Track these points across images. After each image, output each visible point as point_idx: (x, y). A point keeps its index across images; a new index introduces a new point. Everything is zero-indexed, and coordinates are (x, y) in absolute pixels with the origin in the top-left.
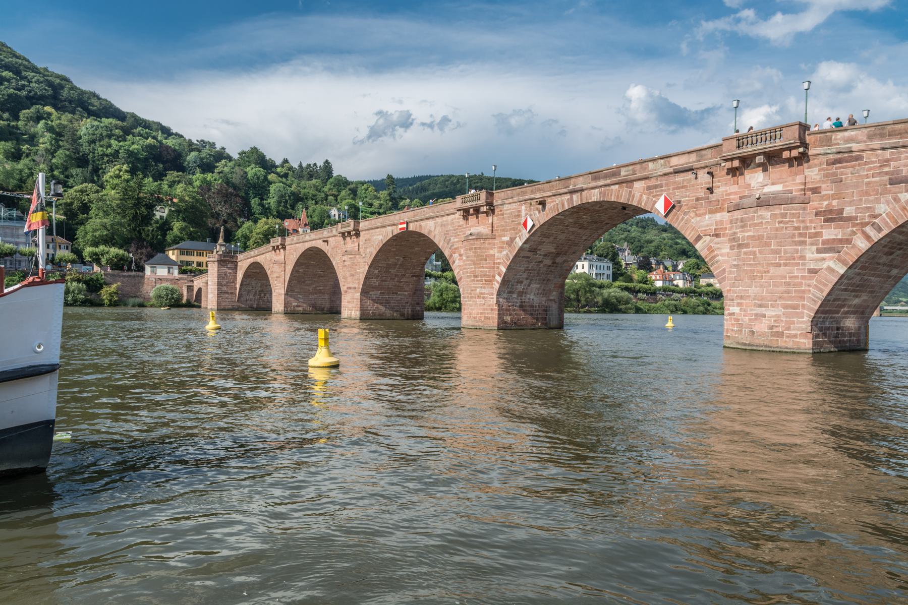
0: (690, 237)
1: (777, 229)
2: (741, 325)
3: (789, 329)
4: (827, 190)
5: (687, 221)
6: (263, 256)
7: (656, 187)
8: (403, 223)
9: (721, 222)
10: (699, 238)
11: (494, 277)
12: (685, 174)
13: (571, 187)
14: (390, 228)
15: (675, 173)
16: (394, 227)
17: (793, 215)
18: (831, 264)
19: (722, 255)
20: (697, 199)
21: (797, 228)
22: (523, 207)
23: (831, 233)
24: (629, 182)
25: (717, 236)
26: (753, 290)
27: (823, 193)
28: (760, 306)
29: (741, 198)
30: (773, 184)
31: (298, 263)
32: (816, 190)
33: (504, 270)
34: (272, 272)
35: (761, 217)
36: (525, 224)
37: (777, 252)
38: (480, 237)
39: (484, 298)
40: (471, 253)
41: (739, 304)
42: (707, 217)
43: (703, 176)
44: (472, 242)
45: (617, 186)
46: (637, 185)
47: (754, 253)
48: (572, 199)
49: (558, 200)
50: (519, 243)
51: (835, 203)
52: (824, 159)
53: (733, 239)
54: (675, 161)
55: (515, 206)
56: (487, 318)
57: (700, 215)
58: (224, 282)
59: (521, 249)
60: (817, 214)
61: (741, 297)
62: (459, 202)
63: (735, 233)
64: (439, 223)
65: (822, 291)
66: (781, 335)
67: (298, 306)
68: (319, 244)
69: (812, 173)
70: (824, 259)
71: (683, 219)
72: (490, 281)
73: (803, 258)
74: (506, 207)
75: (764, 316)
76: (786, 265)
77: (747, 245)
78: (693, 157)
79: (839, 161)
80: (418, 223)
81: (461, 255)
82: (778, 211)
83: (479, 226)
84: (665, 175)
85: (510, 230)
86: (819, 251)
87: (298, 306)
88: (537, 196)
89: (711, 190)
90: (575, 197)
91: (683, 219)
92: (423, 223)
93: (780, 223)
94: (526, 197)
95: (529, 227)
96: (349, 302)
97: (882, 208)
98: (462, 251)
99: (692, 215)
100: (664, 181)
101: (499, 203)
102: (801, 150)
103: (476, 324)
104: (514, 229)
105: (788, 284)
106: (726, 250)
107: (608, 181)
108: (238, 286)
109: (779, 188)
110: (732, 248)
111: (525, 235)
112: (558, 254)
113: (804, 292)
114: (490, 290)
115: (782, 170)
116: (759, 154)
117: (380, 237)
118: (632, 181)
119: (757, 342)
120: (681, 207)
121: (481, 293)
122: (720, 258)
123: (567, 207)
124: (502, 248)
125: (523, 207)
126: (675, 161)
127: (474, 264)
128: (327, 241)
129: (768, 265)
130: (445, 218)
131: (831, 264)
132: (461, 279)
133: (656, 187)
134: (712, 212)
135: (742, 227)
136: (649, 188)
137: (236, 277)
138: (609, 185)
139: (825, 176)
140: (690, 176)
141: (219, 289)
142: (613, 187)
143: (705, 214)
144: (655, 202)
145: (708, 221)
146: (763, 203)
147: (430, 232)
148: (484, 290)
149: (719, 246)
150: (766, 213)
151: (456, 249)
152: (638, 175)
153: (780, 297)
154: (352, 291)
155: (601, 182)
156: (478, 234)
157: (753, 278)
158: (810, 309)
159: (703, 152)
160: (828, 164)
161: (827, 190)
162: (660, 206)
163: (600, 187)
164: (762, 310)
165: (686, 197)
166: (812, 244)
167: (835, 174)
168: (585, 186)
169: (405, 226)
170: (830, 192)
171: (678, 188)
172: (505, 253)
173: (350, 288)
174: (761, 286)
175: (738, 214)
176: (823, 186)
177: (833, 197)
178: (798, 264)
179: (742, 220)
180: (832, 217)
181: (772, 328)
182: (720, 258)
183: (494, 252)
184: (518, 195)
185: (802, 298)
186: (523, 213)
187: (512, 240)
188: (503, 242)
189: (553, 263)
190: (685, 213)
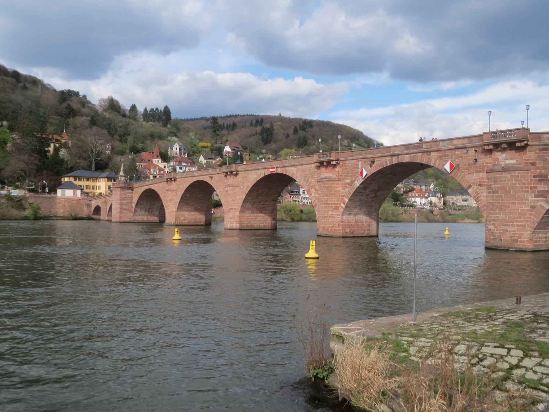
0: (465, 185)
1: (514, 184)
2: (495, 236)
3: (520, 238)
4: (539, 164)
5: (463, 177)
6: (157, 185)
7: (445, 156)
8: (274, 168)
9: (483, 178)
10: (470, 186)
11: (340, 204)
12: (462, 150)
13: (391, 153)
14: (263, 171)
15: (456, 149)
16: (265, 170)
17: (522, 177)
18: (542, 203)
19: (483, 196)
20: (469, 165)
21: (524, 184)
22: (360, 163)
24: (428, 152)
25: (480, 185)
26: (501, 216)
27: (537, 165)
28: (505, 225)
29: (493, 166)
30: (511, 159)
31: (188, 190)
32: (533, 164)
33: (347, 200)
34: (164, 196)
35: (505, 177)
36: (361, 173)
37: (514, 196)
38: (330, 180)
39: (333, 217)
41: (493, 224)
42: (474, 175)
43: (472, 152)
44: (325, 182)
45: (420, 154)
46: (433, 154)
47: (502, 196)
48: (392, 160)
49: (383, 160)
50: (357, 184)
51: (543, 171)
52: (537, 147)
53: (489, 188)
54: (455, 142)
55: (354, 161)
56: (336, 230)
57: (471, 174)
58: (124, 202)
59: (358, 188)
60: (535, 177)
61: (495, 220)
62: (316, 158)
63: (491, 185)
64: (298, 167)
65: (537, 218)
66: (516, 241)
67: (184, 220)
68: (206, 179)
69: (531, 154)
70: (538, 201)
71: (460, 175)
72: (338, 207)
73: (527, 200)
74: (348, 162)
75: (507, 231)
76: (518, 203)
77: (497, 192)
78: (466, 141)
79: (545, 149)
80: (284, 169)
81: (316, 190)
82: (515, 174)
84: (450, 149)
85: (351, 176)
86: (536, 196)
87: (184, 220)
88: (369, 156)
89: (476, 160)
90: (394, 158)
91: (460, 175)
92: (288, 169)
93: (515, 180)
94: (361, 157)
95: (364, 175)
96: (231, 218)
99: (466, 173)
100: (449, 153)
101: (344, 159)
102: (526, 142)
103: (329, 234)
104: (353, 176)
105: (520, 214)
107: (415, 151)
108: (134, 205)
109: (513, 161)
110: (489, 193)
111: (361, 181)
112: (378, 191)
113: (528, 218)
114: (338, 213)
116: (503, 143)
117: (255, 176)
118: (430, 152)
119: (503, 245)
120: (459, 168)
121: (332, 215)
122: (482, 198)
123: (389, 165)
124: (346, 187)
125: (360, 163)
126: (455, 142)
127: (327, 196)
128: (212, 178)
129: (509, 203)
130: (304, 167)
131: (542, 203)
132: (316, 205)
133: (445, 156)
134: (478, 172)
135: (495, 182)
136: (440, 156)
137: (132, 199)
138: (416, 153)
139: (539, 157)
140: (464, 151)
141: (121, 207)
142: (418, 154)
143: (473, 173)
144: (444, 165)
145: (475, 177)
146: (506, 169)
147: (293, 174)
148: (333, 213)
149: (481, 191)
150: (507, 175)
151: (312, 186)
152: (434, 149)
153: (516, 221)
154: (234, 211)
155: (411, 151)
156: (329, 178)
158: (531, 227)
159: (472, 139)
160: (540, 150)
161: (539, 164)
162: (447, 167)
163: (410, 154)
164: (506, 228)
165: (462, 163)
166: (532, 192)
167: (543, 156)
168: (400, 153)
169: (274, 170)
170: (541, 165)
171: (457, 158)
172: (347, 190)
173: (232, 209)
174: (506, 214)
175: (492, 175)
176: (538, 162)
177: (543, 168)
178: (525, 203)
179: (495, 178)
181: (512, 237)
182: (482, 198)
183: (340, 189)
184: (356, 155)
185: (527, 221)
186: (360, 166)
188: (346, 183)
189: (376, 195)
190: (462, 172)
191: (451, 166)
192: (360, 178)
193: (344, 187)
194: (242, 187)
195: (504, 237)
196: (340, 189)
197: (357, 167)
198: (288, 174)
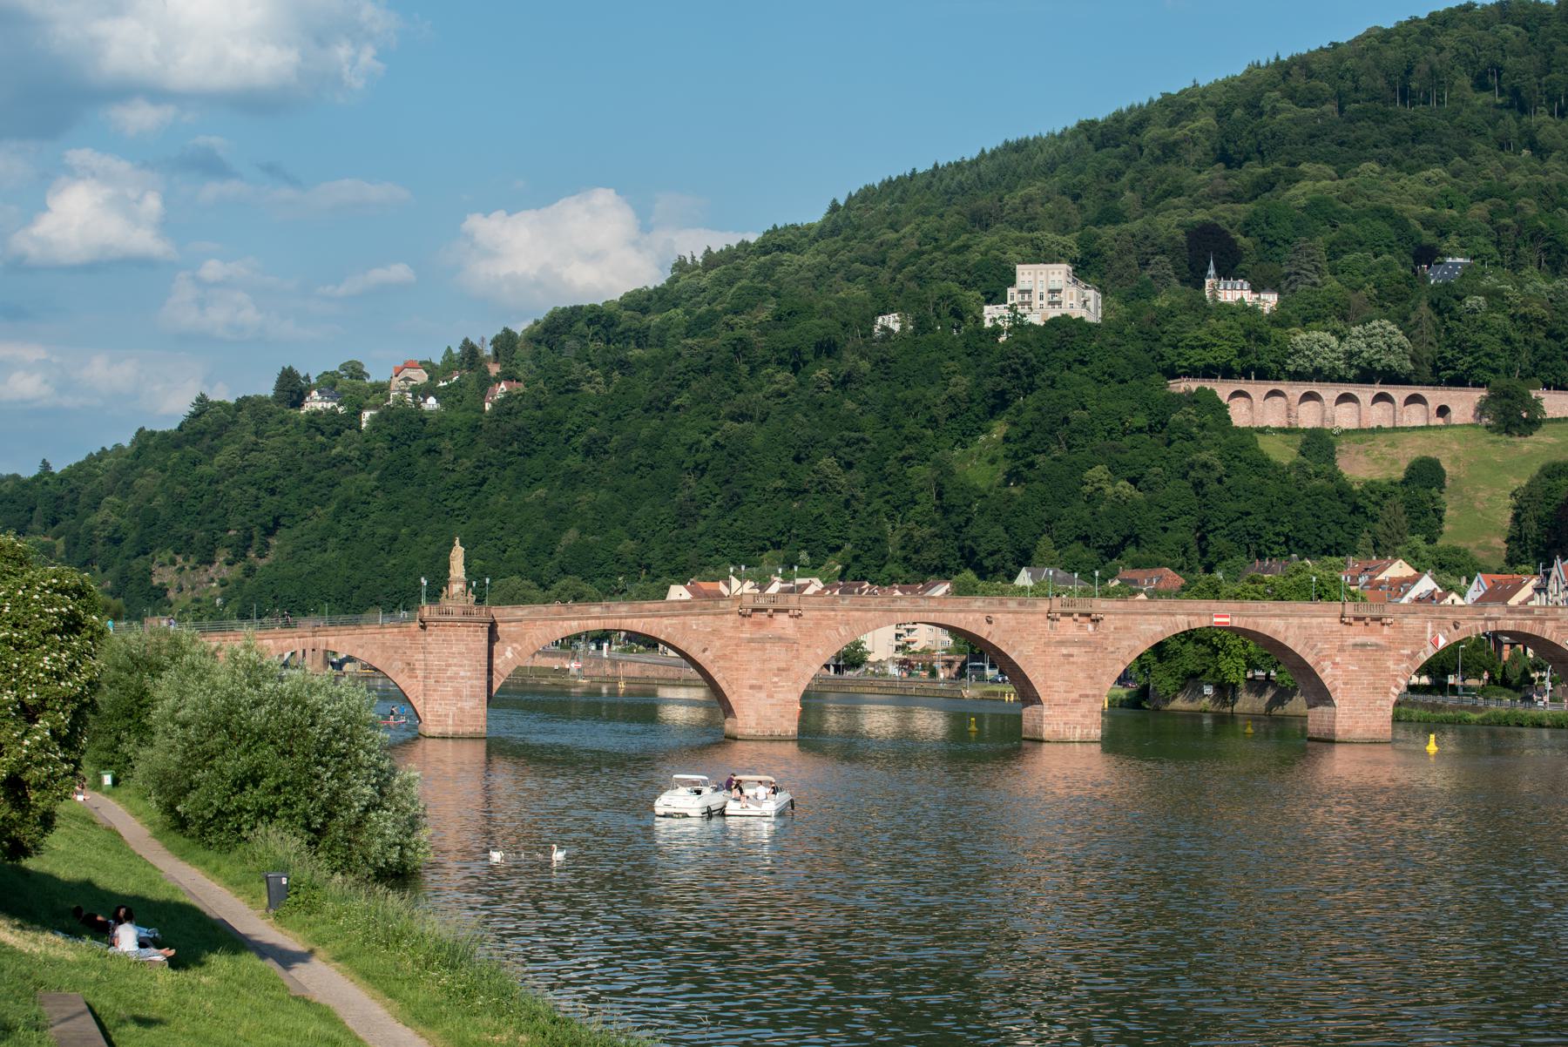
6: (666, 621)
16: (1192, 618)
36: (1437, 641)
40: (1369, 664)
49: (1471, 624)
83: (1357, 634)
92: (1261, 621)
98: (1338, 659)
117: (1159, 628)
130: (1305, 620)
183: (1391, 664)
186: (1429, 630)
187: (1414, 654)
192: (1430, 647)
193: (1399, 661)
194: (1111, 649)
196: (1391, 664)
197: (1424, 631)
198: (1260, 630)
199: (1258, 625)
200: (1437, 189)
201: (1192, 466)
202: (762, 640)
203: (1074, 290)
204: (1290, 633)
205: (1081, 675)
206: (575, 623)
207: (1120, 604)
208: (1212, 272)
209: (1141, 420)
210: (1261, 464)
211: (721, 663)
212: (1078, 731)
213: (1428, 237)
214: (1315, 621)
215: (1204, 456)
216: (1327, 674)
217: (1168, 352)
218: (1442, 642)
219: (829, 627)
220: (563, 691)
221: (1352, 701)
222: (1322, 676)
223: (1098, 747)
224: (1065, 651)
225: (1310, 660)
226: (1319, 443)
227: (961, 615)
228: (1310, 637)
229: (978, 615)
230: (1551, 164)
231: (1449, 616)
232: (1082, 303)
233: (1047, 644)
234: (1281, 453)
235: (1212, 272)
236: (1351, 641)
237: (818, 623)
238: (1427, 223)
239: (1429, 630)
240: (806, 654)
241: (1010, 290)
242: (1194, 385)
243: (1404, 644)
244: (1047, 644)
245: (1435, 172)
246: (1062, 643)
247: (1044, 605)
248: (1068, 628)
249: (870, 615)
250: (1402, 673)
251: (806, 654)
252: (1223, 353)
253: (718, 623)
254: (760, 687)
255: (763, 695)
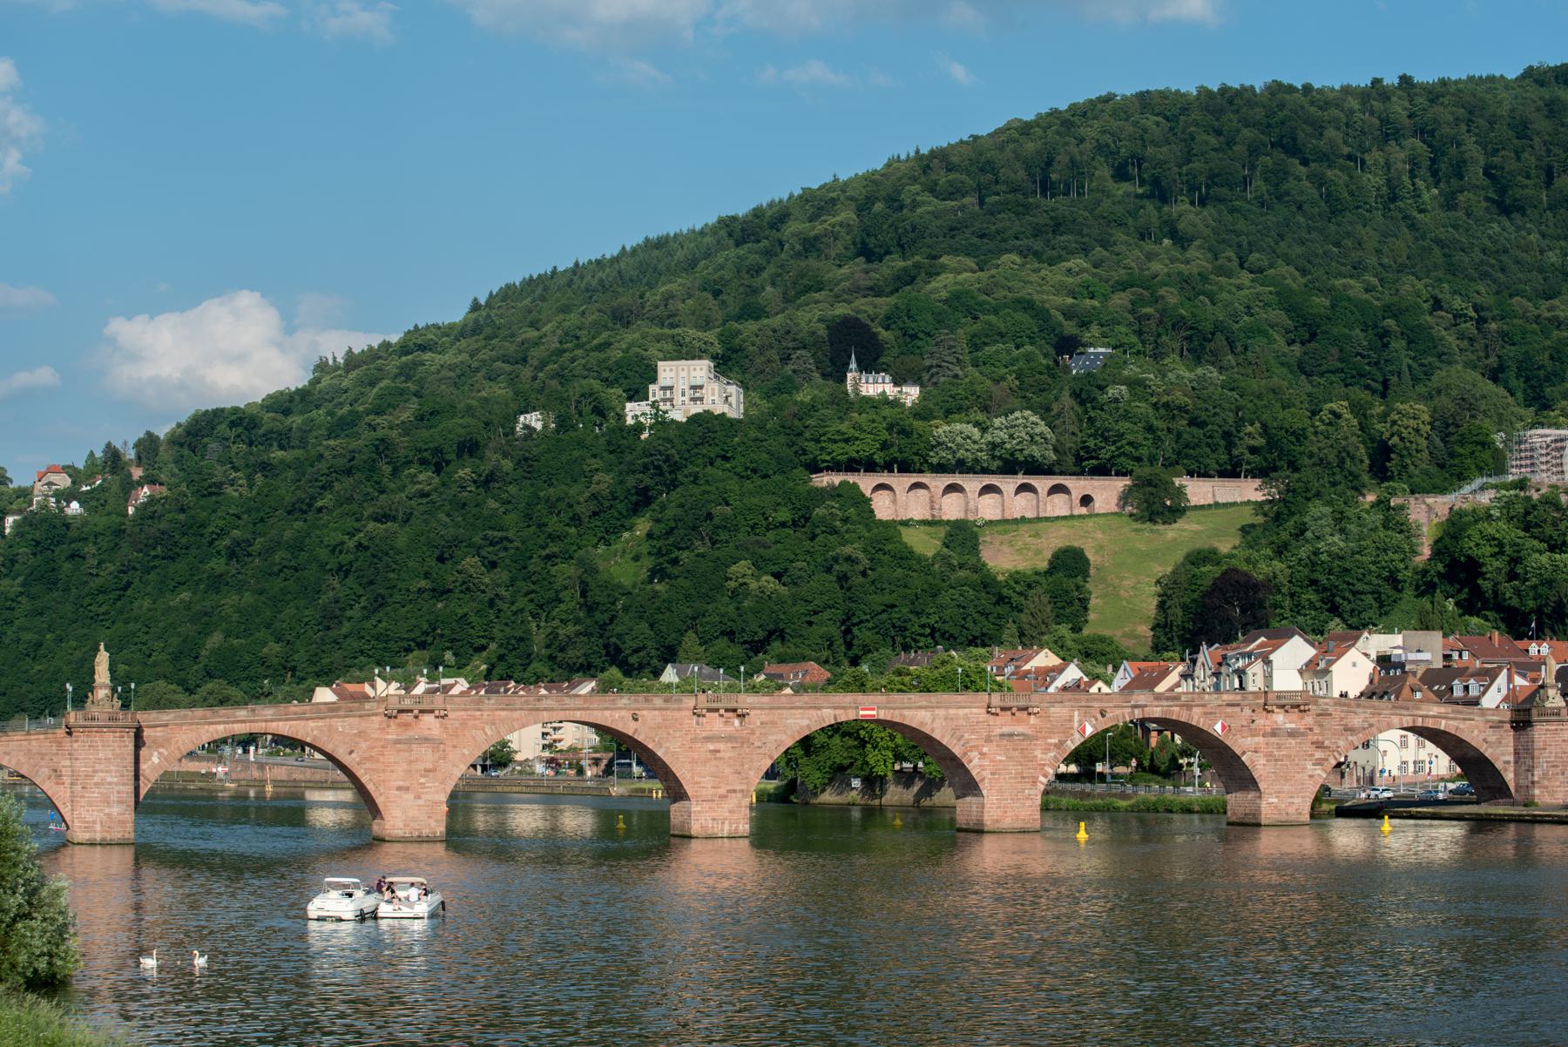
6: (311, 724)
16: (838, 712)
23: (1319, 755)
43: (1247, 711)
49: (1118, 712)
53: (1269, 756)
69: (1309, 720)
83: (1004, 724)
92: (907, 713)
97: (1341, 743)
98: (985, 750)
106: (1263, 761)
115: (1295, 714)
117: (806, 722)
130: (951, 711)
147: (922, 723)
157: (1286, 780)
162: (1218, 727)
180: (1319, 745)
183: (1038, 753)
186: (1076, 719)
187: (1062, 743)
191: (1224, 727)
192: (1077, 735)
195: (1291, 810)
197: (1071, 720)
199: (904, 717)
200: (1078, 280)
201: (836, 560)
202: (409, 742)
203: (716, 386)
204: (938, 724)
205: (728, 770)
206: (221, 727)
207: (766, 699)
208: (853, 366)
209: (784, 515)
210: (905, 557)
211: (368, 765)
212: (726, 827)
213: (1070, 328)
214: (961, 712)
215: (848, 550)
216: (975, 765)
217: (811, 446)
218: (1089, 730)
219: (475, 727)
220: (211, 796)
221: (1000, 791)
222: (969, 767)
223: (746, 842)
224: (711, 747)
225: (957, 751)
226: (963, 535)
227: (607, 713)
228: (957, 728)
229: (624, 713)
230: (1192, 253)
231: (1096, 704)
232: (723, 399)
233: (694, 740)
234: (925, 545)
235: (853, 366)
236: (998, 731)
237: (464, 723)
238: (1068, 314)
239: (1076, 719)
240: (453, 755)
241: (651, 387)
242: (836, 479)
243: (1051, 733)
244: (694, 740)
245: (1077, 262)
246: (708, 739)
247: (690, 702)
248: (715, 724)
249: (516, 714)
250: (1050, 762)
251: (453, 755)
252: (866, 447)
253: (363, 724)
254: (407, 789)
255: (410, 796)
